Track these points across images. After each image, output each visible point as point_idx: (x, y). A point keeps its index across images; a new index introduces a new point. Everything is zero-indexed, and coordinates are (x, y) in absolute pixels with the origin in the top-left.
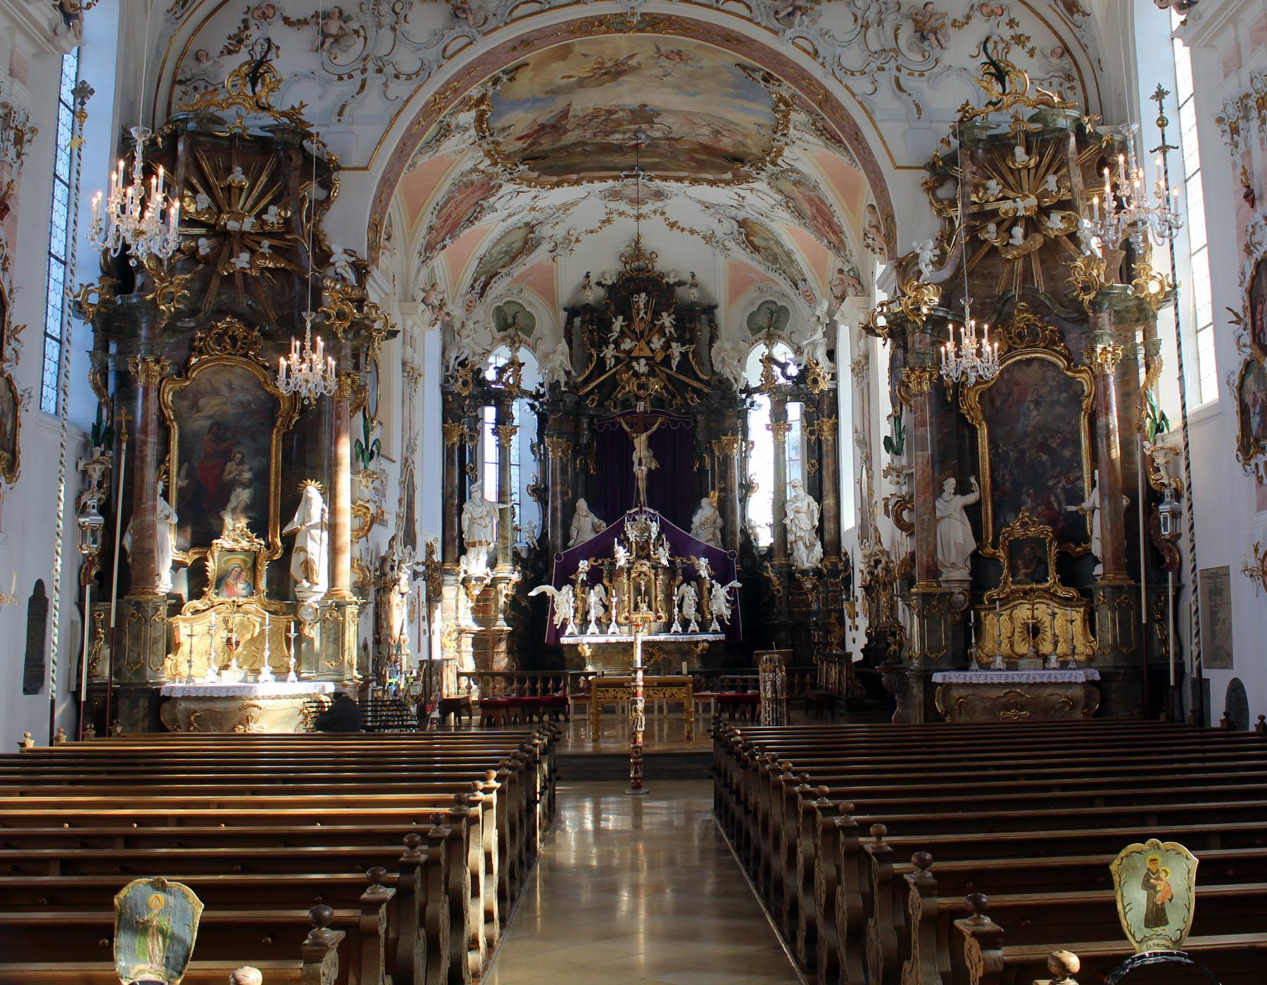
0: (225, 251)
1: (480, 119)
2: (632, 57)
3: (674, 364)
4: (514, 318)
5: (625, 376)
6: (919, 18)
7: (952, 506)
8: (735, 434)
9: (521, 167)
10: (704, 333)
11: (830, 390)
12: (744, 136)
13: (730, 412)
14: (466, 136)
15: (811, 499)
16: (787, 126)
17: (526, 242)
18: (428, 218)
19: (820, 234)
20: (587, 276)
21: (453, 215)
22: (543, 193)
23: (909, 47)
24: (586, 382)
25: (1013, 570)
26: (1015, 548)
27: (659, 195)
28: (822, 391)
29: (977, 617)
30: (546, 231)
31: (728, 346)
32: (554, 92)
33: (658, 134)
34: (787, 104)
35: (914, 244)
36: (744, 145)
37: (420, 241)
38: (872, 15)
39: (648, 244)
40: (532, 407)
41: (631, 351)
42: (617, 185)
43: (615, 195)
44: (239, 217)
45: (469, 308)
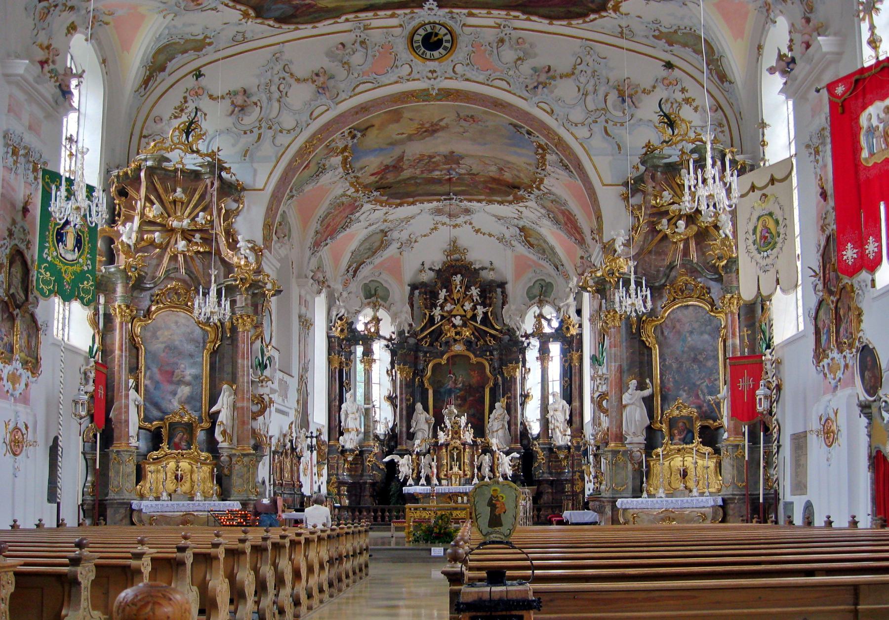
0: (173, 241)
1: (345, 161)
2: (442, 120)
3: (479, 319)
4: (376, 291)
5: (447, 327)
6: (621, 88)
7: (632, 396)
8: (517, 362)
9: (375, 193)
11: (577, 334)
12: (518, 171)
13: (515, 349)
14: (337, 173)
15: (565, 402)
16: (544, 164)
17: (382, 242)
18: (314, 225)
20: (423, 264)
22: (391, 210)
23: (614, 107)
24: (422, 330)
25: (672, 437)
26: (672, 423)
27: (467, 211)
28: (572, 335)
29: (648, 466)
30: (395, 235)
32: (393, 144)
34: (543, 149)
35: (612, 233)
36: (519, 177)
37: (309, 241)
38: (590, 88)
39: (463, 242)
40: (387, 346)
41: (451, 311)
42: (440, 205)
43: (438, 212)
44: (181, 220)
45: (346, 285)
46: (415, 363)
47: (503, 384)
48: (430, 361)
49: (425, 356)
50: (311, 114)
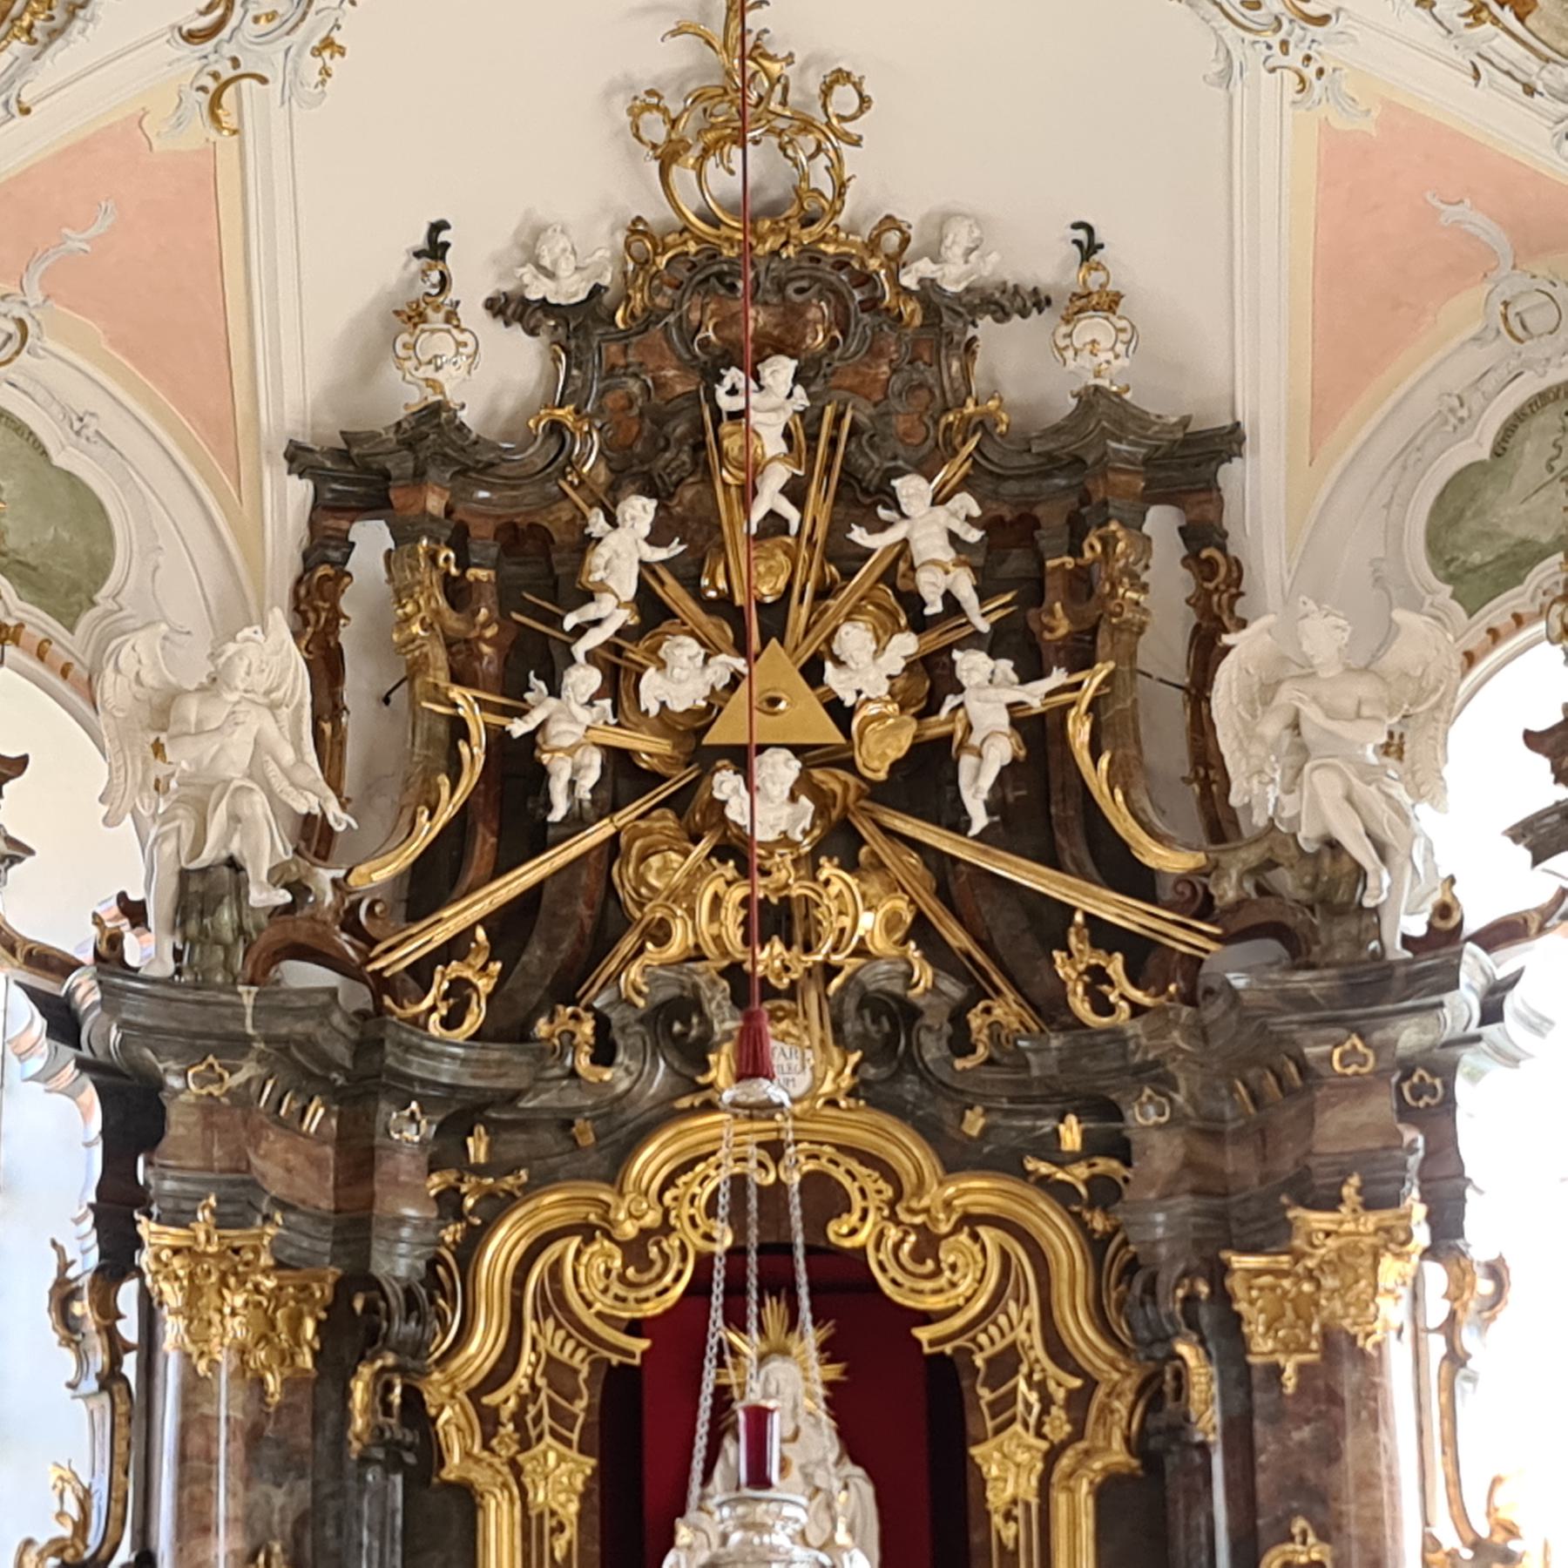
3: (976, 787)
5: (665, 870)
10: (1163, 591)
24: (428, 886)
31: (1324, 637)
46: (354, 1227)
47: (1239, 1431)
48: (497, 1207)
49: (445, 1151)
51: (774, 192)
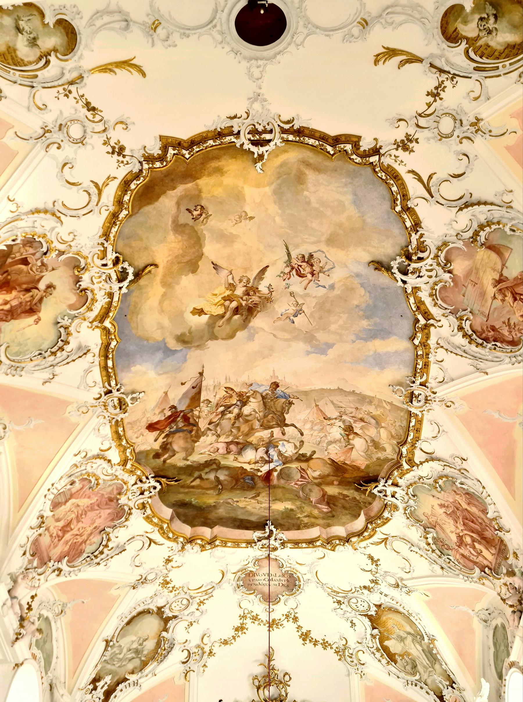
9: (153, 483)
17: (158, 644)
19: (469, 564)
21: (76, 527)
33: (288, 450)
50: (39, 108)
51: (276, 696)
